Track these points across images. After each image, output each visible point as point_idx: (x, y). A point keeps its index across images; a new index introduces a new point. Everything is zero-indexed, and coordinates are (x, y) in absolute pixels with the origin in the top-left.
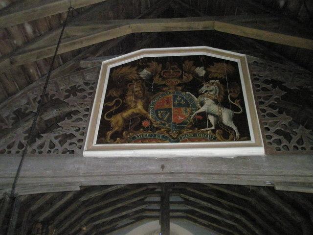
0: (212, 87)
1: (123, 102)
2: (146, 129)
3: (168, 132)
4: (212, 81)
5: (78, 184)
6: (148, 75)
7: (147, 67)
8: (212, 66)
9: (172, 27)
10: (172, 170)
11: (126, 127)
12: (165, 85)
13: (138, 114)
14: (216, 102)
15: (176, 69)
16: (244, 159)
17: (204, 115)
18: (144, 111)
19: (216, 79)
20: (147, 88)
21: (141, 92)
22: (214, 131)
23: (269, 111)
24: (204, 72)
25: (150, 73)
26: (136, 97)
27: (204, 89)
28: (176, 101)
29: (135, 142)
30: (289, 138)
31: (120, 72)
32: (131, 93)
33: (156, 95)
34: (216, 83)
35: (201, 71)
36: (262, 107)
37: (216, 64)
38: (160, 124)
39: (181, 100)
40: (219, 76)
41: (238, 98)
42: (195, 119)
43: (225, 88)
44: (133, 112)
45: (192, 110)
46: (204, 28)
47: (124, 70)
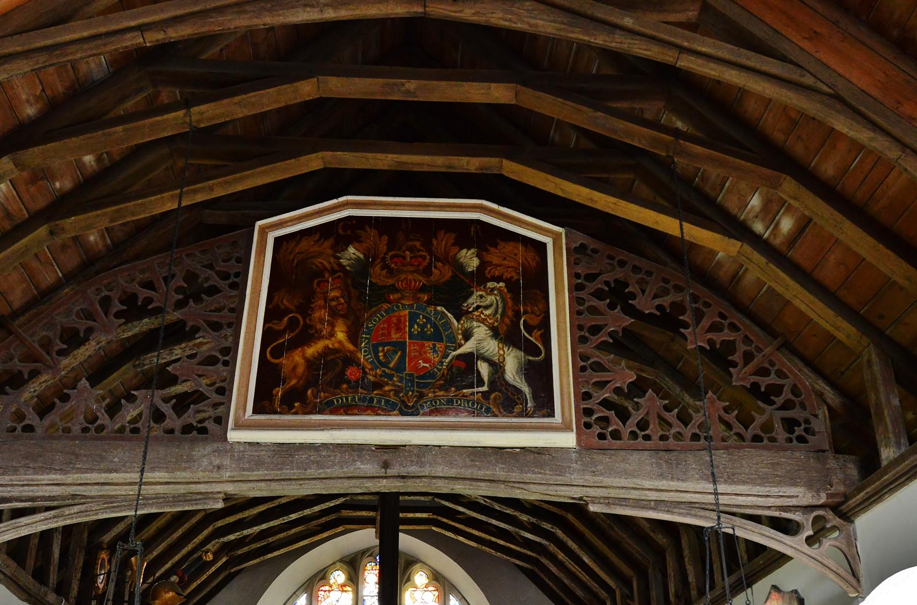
0: (490, 299)
4: (490, 285)
5: (220, 496)
6: (358, 259)
8: (492, 249)
9: (412, 164)
10: (403, 471)
11: (311, 380)
13: (335, 351)
14: (495, 333)
15: (419, 250)
16: (538, 453)
17: (470, 359)
18: (350, 347)
19: (498, 279)
21: (342, 300)
24: (475, 262)
25: (362, 256)
26: (334, 314)
27: (473, 301)
28: (416, 327)
29: (333, 412)
30: (624, 416)
31: (297, 250)
32: (321, 302)
33: (374, 309)
34: (499, 289)
35: (470, 260)
36: (582, 349)
37: (502, 244)
38: (381, 376)
39: (424, 325)
40: (507, 275)
43: (516, 300)
44: (327, 347)
45: (447, 347)
46: (481, 169)
47: (304, 244)
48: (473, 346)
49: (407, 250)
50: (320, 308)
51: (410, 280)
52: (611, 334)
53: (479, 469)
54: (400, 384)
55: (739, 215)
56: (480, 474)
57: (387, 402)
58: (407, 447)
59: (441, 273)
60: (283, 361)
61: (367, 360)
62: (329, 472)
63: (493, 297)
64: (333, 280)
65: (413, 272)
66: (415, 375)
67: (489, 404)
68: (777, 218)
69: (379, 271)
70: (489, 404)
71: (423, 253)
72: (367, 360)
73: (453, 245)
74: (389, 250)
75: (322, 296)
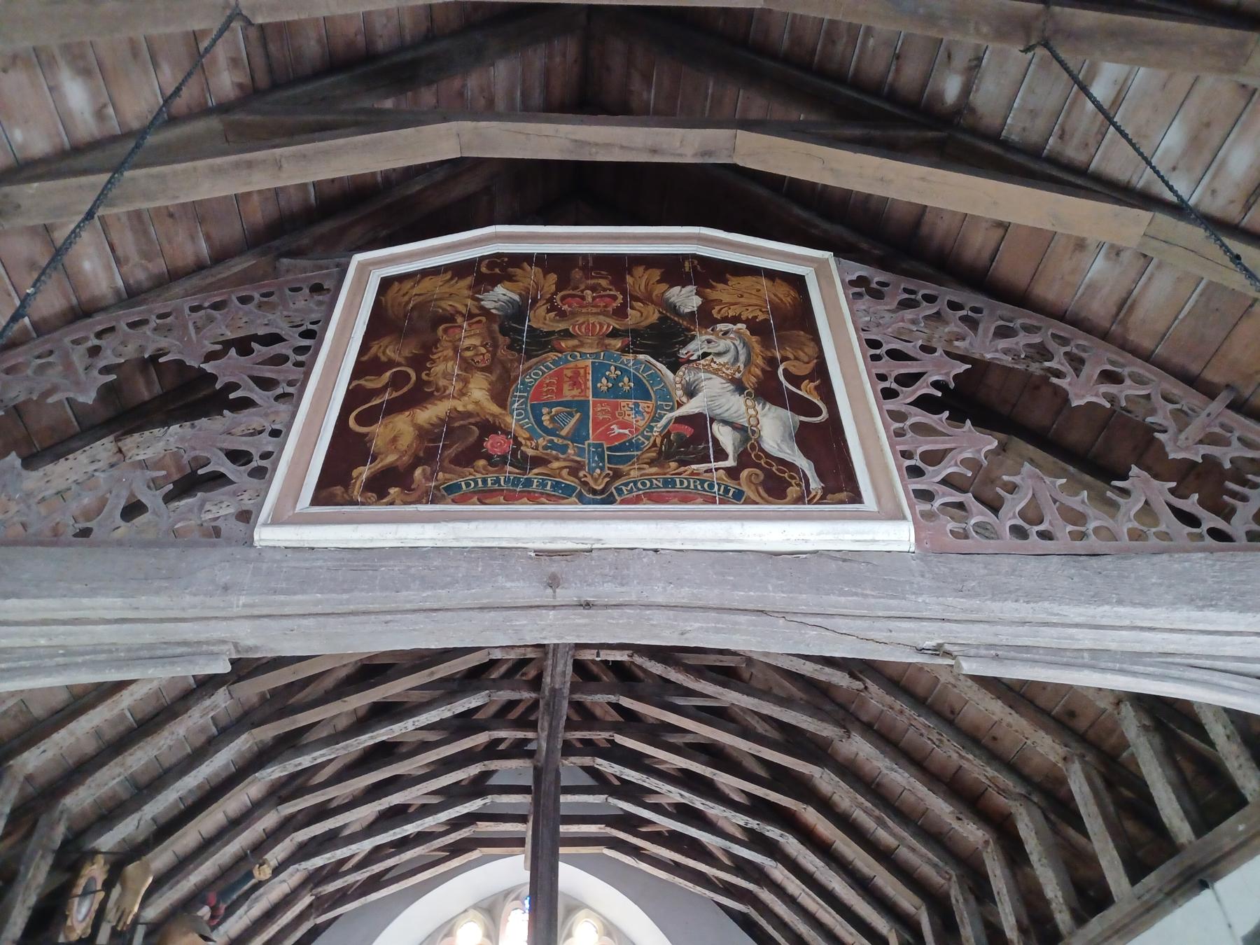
0: (722, 345)
1: (419, 377)
2: (496, 462)
3: (574, 472)
4: (722, 327)
5: (224, 648)
6: (512, 302)
7: (507, 278)
8: (720, 286)
10: (588, 595)
12: (566, 334)
13: (468, 415)
14: (739, 387)
15: (605, 290)
16: (844, 560)
17: (699, 422)
19: (735, 320)
20: (503, 340)
21: (483, 350)
22: (733, 473)
23: (919, 416)
25: (517, 298)
26: (468, 366)
27: (695, 348)
28: (604, 380)
29: (455, 502)
31: (415, 291)
32: (450, 353)
33: (534, 360)
34: (738, 332)
35: (686, 298)
37: (733, 281)
38: (545, 448)
39: (618, 379)
41: (810, 377)
42: (669, 433)
43: (766, 343)
45: (657, 407)
48: (703, 404)
49: (587, 288)
50: (446, 359)
51: (593, 324)
52: (936, 385)
53: (735, 587)
54: (579, 459)
55: (1134, 180)
56: (738, 597)
57: (556, 485)
58: (594, 554)
59: (642, 316)
60: (377, 429)
61: (522, 426)
62: (443, 596)
63: (728, 342)
64: (470, 325)
65: (598, 314)
66: (605, 446)
67: (739, 485)
68: (1221, 154)
69: (544, 314)
70: (739, 485)
71: (611, 293)
72: (522, 426)
73: (659, 282)
74: (559, 289)
75: (450, 344)
